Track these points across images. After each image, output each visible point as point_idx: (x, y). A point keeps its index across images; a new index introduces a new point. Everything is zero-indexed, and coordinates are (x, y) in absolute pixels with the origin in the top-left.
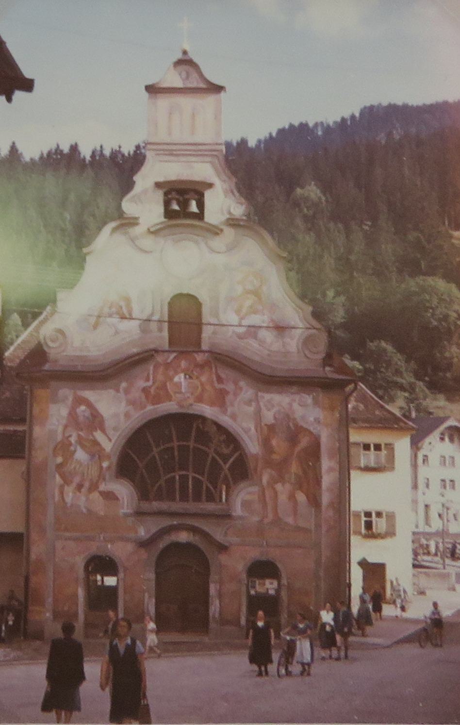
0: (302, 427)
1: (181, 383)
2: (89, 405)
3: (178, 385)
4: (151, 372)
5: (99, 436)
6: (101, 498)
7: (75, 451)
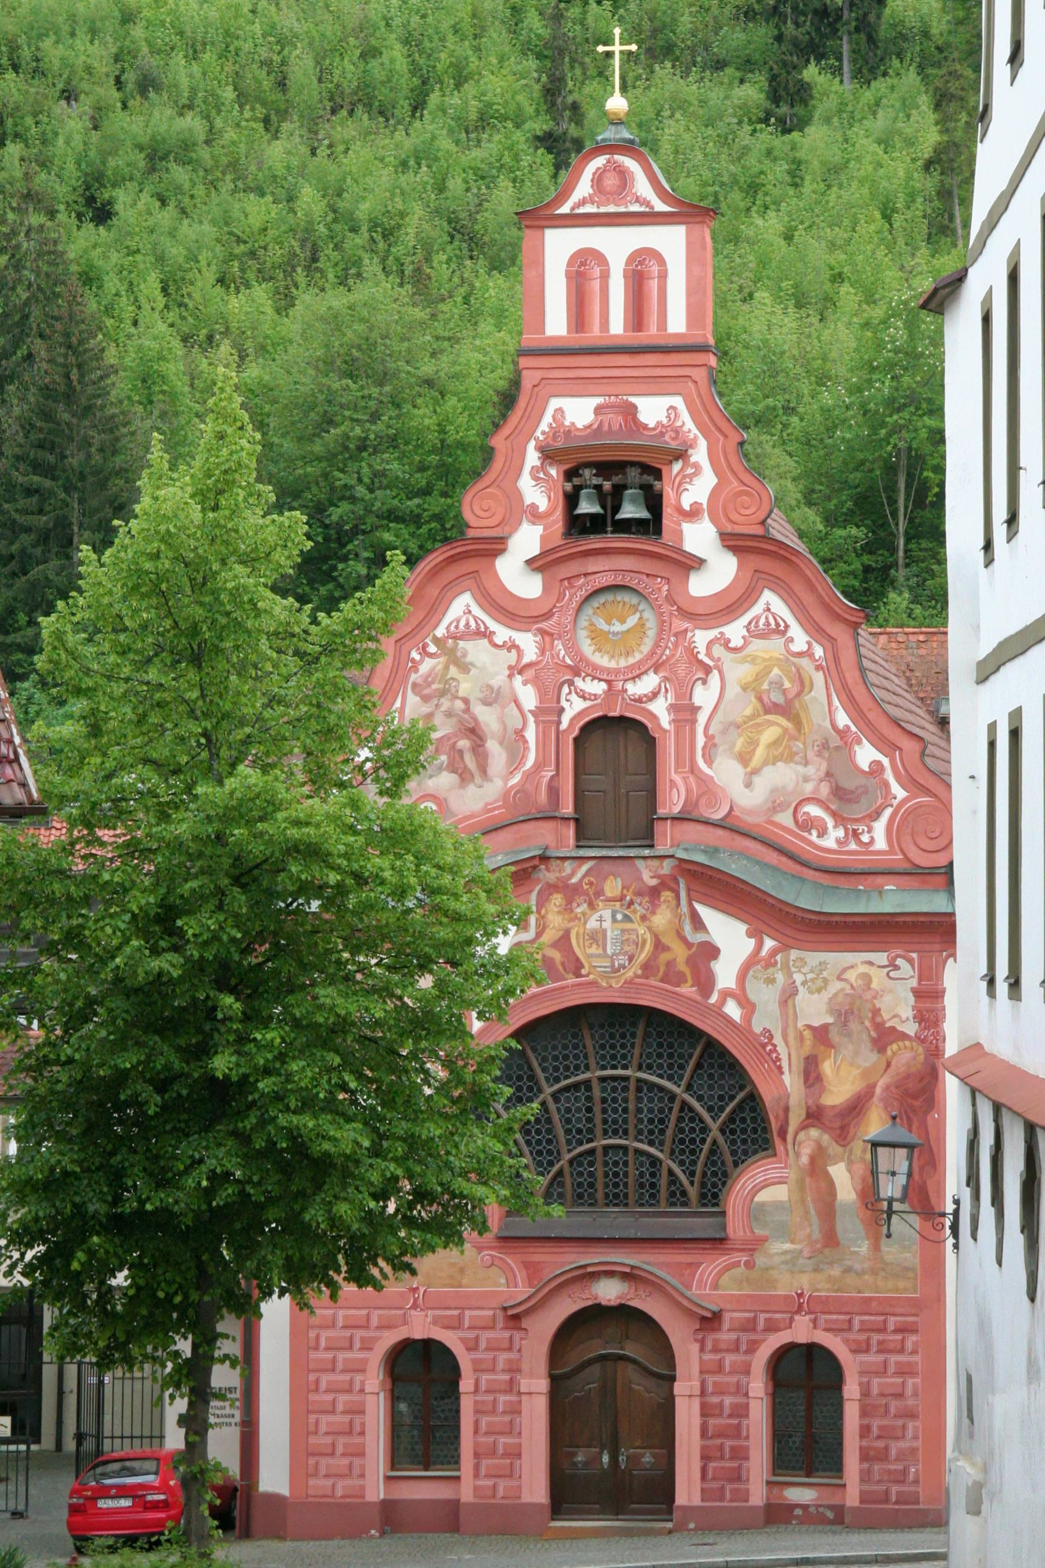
0: (893, 1029)
1: (604, 932)
3: (597, 937)
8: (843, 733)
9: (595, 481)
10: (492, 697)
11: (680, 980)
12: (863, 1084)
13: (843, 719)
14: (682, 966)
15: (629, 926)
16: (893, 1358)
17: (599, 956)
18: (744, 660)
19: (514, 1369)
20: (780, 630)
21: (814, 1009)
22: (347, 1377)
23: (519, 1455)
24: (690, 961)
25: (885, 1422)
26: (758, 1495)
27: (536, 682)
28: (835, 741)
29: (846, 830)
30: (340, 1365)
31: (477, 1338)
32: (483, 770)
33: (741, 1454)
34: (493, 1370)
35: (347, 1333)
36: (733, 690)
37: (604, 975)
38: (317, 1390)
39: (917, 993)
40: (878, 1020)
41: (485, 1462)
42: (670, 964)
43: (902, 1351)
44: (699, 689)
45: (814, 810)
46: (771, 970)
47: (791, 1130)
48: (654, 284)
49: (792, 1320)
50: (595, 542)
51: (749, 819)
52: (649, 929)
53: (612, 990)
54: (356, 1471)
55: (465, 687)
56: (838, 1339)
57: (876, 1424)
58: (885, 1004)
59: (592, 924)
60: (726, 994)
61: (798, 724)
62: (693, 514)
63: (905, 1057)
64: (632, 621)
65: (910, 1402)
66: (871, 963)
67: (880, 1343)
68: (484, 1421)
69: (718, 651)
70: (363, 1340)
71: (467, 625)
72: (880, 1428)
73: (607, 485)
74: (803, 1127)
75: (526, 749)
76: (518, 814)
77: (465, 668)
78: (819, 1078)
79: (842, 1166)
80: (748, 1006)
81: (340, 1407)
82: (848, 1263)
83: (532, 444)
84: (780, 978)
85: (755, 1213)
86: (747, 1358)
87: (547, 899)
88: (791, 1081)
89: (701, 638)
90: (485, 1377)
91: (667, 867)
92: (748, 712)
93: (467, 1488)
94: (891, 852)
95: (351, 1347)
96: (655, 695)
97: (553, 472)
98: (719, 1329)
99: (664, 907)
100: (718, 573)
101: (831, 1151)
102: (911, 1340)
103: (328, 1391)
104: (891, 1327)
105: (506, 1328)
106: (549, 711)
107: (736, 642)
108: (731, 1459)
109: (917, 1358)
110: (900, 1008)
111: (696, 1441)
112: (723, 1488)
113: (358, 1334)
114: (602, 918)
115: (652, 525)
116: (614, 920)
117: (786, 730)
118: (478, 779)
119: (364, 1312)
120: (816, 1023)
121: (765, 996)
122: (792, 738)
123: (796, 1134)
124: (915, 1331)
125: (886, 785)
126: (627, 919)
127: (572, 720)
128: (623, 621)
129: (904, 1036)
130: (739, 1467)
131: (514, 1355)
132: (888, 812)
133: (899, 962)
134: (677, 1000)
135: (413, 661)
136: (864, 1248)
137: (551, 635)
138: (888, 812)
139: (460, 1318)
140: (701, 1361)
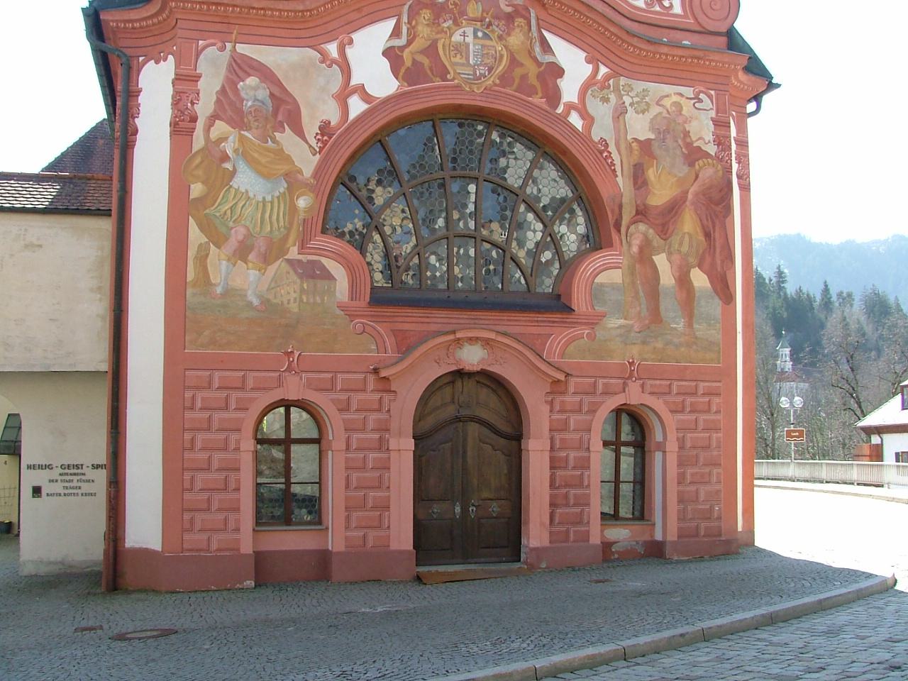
0: (699, 148)
1: (467, 45)
2: (266, 74)
3: (461, 49)
4: (405, 19)
5: (286, 138)
7: (234, 172)
11: (531, 91)
12: (679, 191)
14: (533, 80)
15: (488, 43)
16: (703, 417)
17: (463, 65)
19: (384, 428)
21: (639, 127)
22: (222, 436)
24: (540, 76)
25: (695, 470)
30: (215, 425)
33: (584, 502)
34: (363, 430)
35: (224, 394)
37: (466, 81)
38: (192, 449)
39: (716, 123)
40: (688, 140)
41: (354, 515)
42: (524, 77)
43: (708, 411)
46: (605, 91)
47: (624, 223)
49: (625, 384)
52: (505, 46)
53: (474, 97)
54: (231, 525)
56: (661, 400)
57: (689, 471)
58: (693, 127)
59: (457, 38)
60: (570, 107)
63: (708, 173)
65: (715, 453)
67: (692, 404)
70: (238, 400)
72: (692, 475)
79: (664, 256)
81: (215, 465)
82: (669, 337)
84: (612, 97)
85: (596, 293)
86: (588, 417)
87: (418, 14)
90: (355, 436)
93: (335, 539)
94: (685, 16)
95: (227, 408)
98: (564, 393)
99: (517, 30)
101: (655, 244)
102: (716, 400)
103: (203, 449)
104: (701, 391)
108: (575, 505)
109: (720, 417)
110: (702, 130)
111: (546, 491)
112: (567, 532)
113: (234, 395)
114: (465, 35)
116: (475, 36)
120: (642, 138)
121: (602, 111)
123: (628, 228)
124: (718, 394)
126: (486, 36)
129: (707, 155)
130: (582, 511)
131: (383, 416)
134: (529, 109)
136: (680, 325)
139: (333, 380)
140: (551, 421)
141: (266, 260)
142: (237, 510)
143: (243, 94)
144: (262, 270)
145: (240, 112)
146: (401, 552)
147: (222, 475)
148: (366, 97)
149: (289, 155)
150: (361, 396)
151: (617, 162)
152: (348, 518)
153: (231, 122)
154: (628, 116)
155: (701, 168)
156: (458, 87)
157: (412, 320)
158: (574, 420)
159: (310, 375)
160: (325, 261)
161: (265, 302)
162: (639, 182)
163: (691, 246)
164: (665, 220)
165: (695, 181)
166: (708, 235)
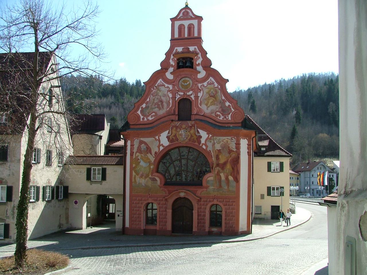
0: (232, 150)
2: (146, 144)
3: (181, 135)
4: (170, 130)
5: (149, 155)
6: (150, 181)
8: (223, 100)
9: (182, 60)
10: (165, 96)
11: (195, 142)
13: (223, 98)
14: (195, 139)
15: (186, 133)
17: (181, 138)
18: (207, 88)
19: (166, 208)
20: (213, 83)
21: (218, 147)
23: (167, 222)
26: (207, 229)
27: (172, 93)
28: (222, 101)
29: (224, 116)
31: (160, 203)
32: (163, 107)
36: (205, 93)
39: (236, 144)
40: (229, 148)
42: (193, 139)
44: (199, 93)
45: (218, 113)
48: (192, 29)
50: (182, 69)
51: (207, 115)
55: (160, 94)
58: (230, 146)
59: (180, 132)
60: (203, 144)
61: (216, 98)
62: (199, 65)
63: (234, 155)
64: (188, 83)
66: (228, 139)
68: (161, 216)
69: (202, 87)
71: (161, 84)
73: (184, 61)
74: (216, 167)
75: (170, 104)
76: (168, 114)
77: (160, 91)
78: (219, 159)
80: (207, 146)
83: (172, 55)
84: (212, 141)
85: (208, 182)
88: (214, 159)
89: (199, 85)
90: (161, 209)
91: (193, 122)
92: (207, 97)
94: (232, 120)
96: (191, 95)
97: (175, 59)
98: (200, 202)
100: (202, 74)
105: (164, 201)
106: (174, 98)
107: (206, 85)
110: (233, 146)
114: (182, 132)
115: (191, 67)
117: (214, 100)
118: (162, 109)
119: (141, 198)
120: (218, 149)
121: (210, 145)
122: (215, 101)
123: (215, 168)
125: (231, 109)
127: (178, 99)
128: (187, 83)
132: (231, 113)
133: (233, 138)
135: (152, 90)
137: (174, 85)
138: (231, 113)
140: (198, 207)
141: (146, 178)
142: (141, 221)
143: (142, 148)
144: (145, 180)
145: (141, 151)
146: (169, 230)
147: (138, 216)
148: (163, 146)
149: (149, 159)
150: (162, 202)
151: (213, 155)
152: (160, 224)
153: (139, 153)
154: (215, 145)
155: (232, 154)
156: (181, 143)
157: (171, 188)
158: (202, 207)
159: (154, 198)
160: (155, 177)
161: (146, 185)
162: (218, 158)
163: (229, 171)
164: (223, 166)
165: (230, 157)
166: (233, 169)
